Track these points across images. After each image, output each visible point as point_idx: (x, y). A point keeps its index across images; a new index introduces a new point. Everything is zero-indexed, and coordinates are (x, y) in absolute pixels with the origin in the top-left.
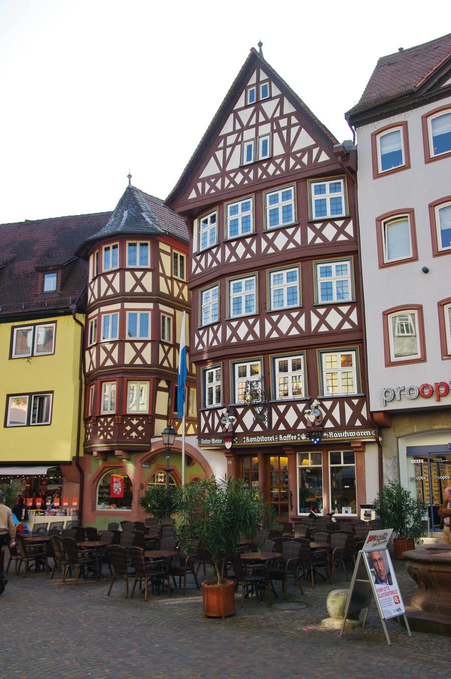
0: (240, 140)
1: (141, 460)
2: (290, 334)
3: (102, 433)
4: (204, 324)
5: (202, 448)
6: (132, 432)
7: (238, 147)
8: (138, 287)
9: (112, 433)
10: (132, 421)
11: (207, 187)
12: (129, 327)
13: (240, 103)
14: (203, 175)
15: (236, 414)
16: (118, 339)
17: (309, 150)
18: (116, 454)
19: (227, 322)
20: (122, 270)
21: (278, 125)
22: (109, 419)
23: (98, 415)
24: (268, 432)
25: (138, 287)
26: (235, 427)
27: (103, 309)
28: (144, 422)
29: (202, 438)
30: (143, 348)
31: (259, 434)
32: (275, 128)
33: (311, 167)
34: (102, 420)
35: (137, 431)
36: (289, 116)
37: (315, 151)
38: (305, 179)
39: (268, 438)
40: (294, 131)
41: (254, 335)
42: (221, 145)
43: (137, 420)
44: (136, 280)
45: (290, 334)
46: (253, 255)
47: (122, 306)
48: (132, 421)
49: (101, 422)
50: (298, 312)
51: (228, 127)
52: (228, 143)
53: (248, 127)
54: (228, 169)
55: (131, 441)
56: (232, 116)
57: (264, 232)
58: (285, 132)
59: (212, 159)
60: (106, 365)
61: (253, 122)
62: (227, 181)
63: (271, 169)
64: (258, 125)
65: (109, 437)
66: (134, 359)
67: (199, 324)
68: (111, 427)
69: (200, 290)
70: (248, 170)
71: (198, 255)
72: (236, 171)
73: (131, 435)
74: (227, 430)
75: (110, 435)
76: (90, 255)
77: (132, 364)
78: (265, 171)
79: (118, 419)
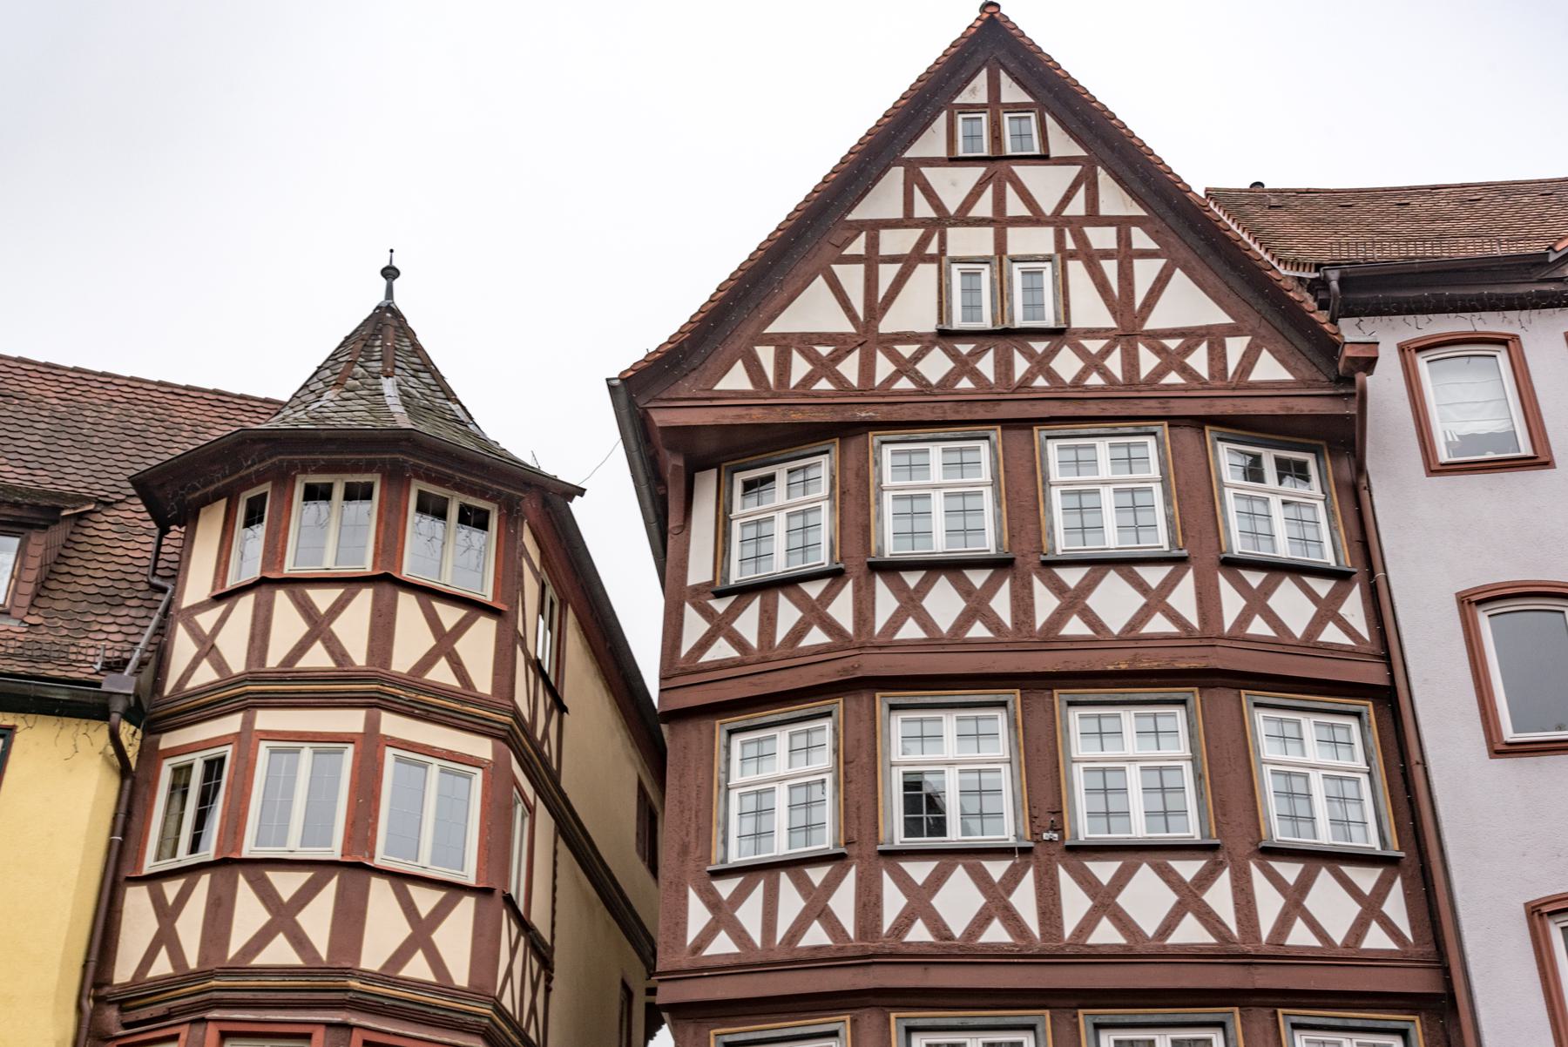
0: (933, 248)
2: (1174, 939)
4: (735, 858)
7: (926, 274)
8: (443, 663)
11: (800, 368)
13: (932, 143)
14: (782, 325)
16: (336, 855)
17: (1214, 337)
20: (387, 581)
21: (1081, 239)
25: (443, 663)
27: (266, 720)
30: (440, 913)
32: (1070, 244)
33: (1226, 388)
36: (1122, 224)
37: (1235, 348)
38: (1199, 422)
40: (1145, 273)
41: (1012, 920)
42: (858, 246)
44: (435, 635)
45: (1174, 939)
46: (999, 630)
47: (372, 725)
50: (1204, 862)
51: (884, 200)
52: (885, 249)
53: (963, 219)
54: (889, 324)
56: (897, 175)
57: (1043, 558)
58: (1110, 268)
59: (820, 281)
60: (260, 960)
61: (984, 207)
62: (884, 368)
63: (1067, 365)
64: (1000, 222)
66: (402, 956)
67: (717, 854)
69: (720, 726)
70: (972, 346)
71: (720, 594)
72: (925, 343)
76: (208, 500)
77: (387, 976)
78: (1041, 365)
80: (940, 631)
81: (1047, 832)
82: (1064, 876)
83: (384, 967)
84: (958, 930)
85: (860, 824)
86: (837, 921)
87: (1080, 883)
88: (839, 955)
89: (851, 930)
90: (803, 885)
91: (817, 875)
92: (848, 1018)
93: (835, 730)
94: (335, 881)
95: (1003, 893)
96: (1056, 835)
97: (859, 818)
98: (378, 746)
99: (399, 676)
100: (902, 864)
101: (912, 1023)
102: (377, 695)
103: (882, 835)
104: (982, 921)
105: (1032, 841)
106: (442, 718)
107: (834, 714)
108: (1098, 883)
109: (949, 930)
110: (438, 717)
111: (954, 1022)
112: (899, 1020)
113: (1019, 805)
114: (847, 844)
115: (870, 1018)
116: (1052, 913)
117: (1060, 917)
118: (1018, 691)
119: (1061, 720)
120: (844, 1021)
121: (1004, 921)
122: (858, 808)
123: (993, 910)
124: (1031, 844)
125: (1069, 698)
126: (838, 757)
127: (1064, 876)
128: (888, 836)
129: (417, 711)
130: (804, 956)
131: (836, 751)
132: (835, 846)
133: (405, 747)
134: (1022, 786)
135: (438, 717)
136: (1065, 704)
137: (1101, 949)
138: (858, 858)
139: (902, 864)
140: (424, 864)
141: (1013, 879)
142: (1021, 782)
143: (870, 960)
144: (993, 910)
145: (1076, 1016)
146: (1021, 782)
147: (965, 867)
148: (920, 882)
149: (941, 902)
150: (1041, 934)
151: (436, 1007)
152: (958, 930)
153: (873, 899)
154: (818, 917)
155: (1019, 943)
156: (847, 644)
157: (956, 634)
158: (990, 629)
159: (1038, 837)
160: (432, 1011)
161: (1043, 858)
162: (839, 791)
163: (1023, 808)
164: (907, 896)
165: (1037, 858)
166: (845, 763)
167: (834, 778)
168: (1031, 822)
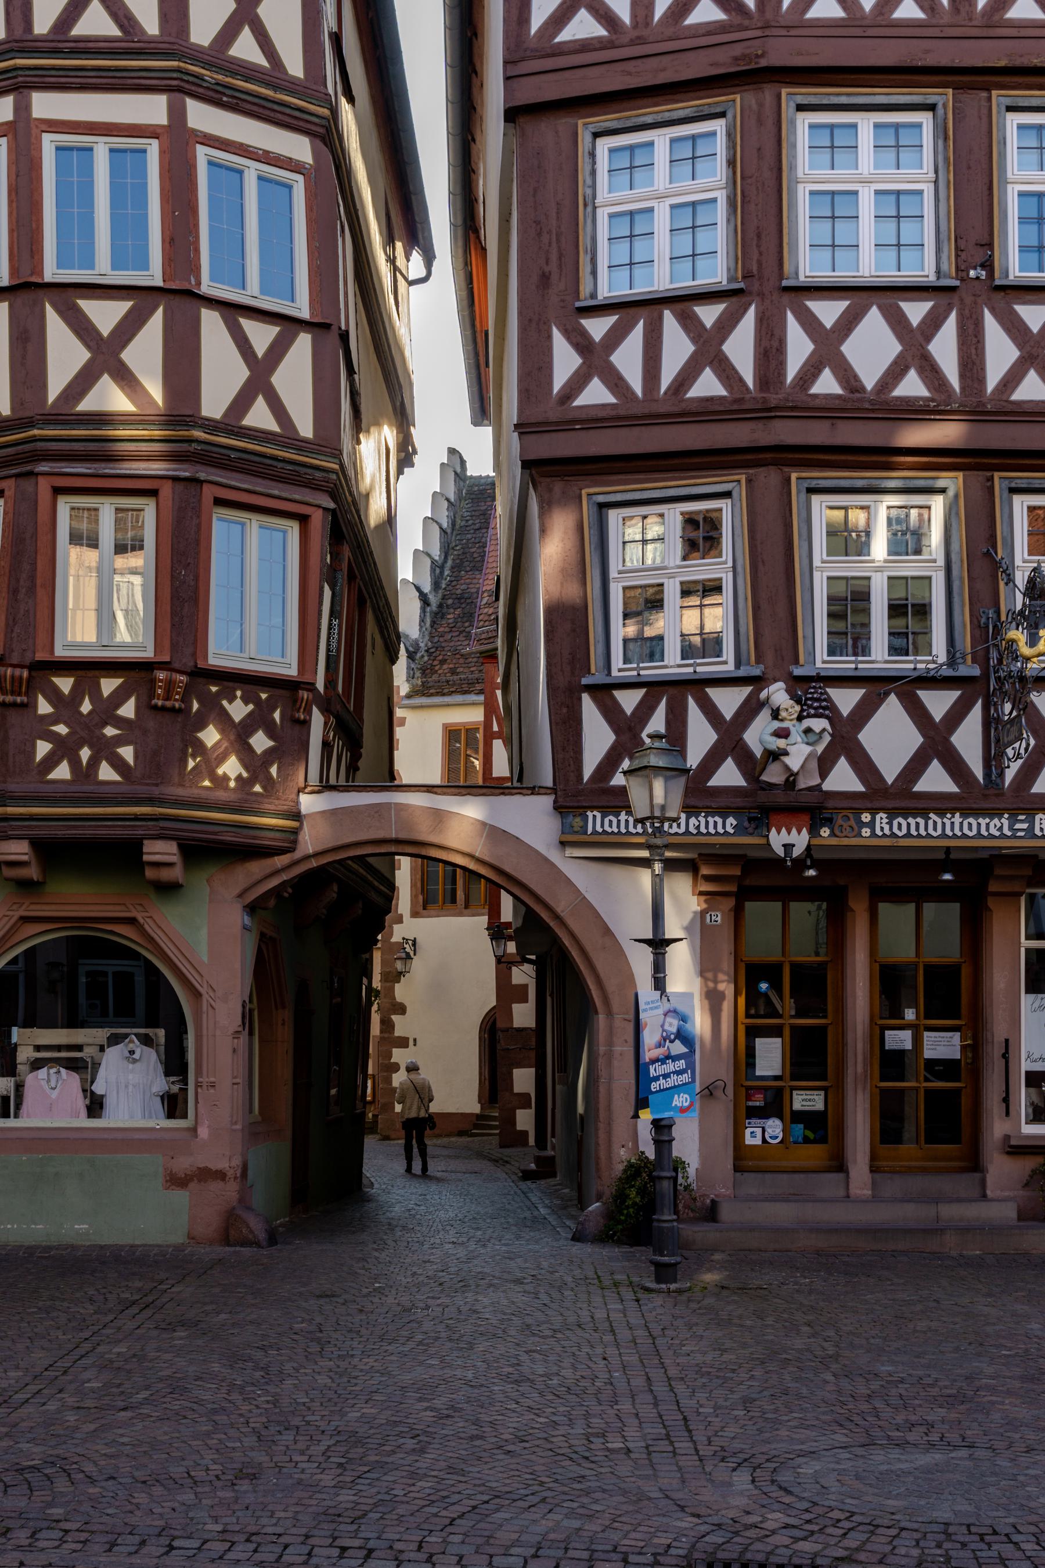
1: (240, 896)
3: (64, 749)
5: (570, 852)
6: (222, 759)
9: (127, 753)
10: (225, 703)
12: (212, 228)
15: (829, 711)
18: (146, 858)
19: (786, 298)
22: (108, 685)
23: (40, 656)
24: (985, 796)
26: (825, 764)
28: (277, 715)
29: (592, 808)
30: (278, 350)
31: (940, 804)
34: (65, 684)
35: (246, 753)
39: (983, 822)
43: (246, 703)
46: (932, 9)
48: (225, 703)
49: (55, 696)
55: (221, 795)
65: (106, 773)
66: (242, 403)
68: (120, 722)
73: (220, 771)
74: (791, 781)
75: (118, 764)
79: (170, 685)
80: (861, 8)
81: (975, 268)
82: (990, 322)
83: (226, 415)
84: (869, 381)
85: (761, 254)
86: (734, 368)
87: (1008, 331)
88: (735, 407)
89: (749, 380)
90: (690, 324)
91: (709, 314)
92: (743, 478)
93: (730, 135)
94: (159, 314)
95: (921, 339)
96: (984, 273)
97: (758, 246)
98: (187, 143)
99: (198, 49)
100: (809, 304)
101: (813, 484)
102: (175, 75)
103: (787, 268)
104: (895, 373)
105: (957, 279)
106: (255, 108)
107: (729, 115)
108: (1027, 329)
109: (860, 381)
110: (248, 106)
111: (860, 484)
112: (800, 481)
113: (944, 236)
114: (744, 277)
115: (769, 477)
116: (974, 363)
117: (983, 369)
118: (950, 91)
119: (998, 130)
120: (739, 481)
121: (921, 372)
122: (759, 236)
123: (910, 359)
124: (957, 283)
125: (1008, 101)
126: (734, 173)
127: (990, 322)
128: (792, 270)
129: (225, 99)
130: (693, 407)
131: (731, 163)
132: (731, 279)
133: (217, 144)
134: (949, 212)
135: (248, 106)
136: (1003, 108)
137: (1025, 406)
138: (758, 295)
139: (809, 304)
140: (252, 293)
141: (933, 324)
142: (949, 206)
143: (773, 414)
144: (910, 359)
145: (991, 479)
146: (949, 206)
147: (880, 308)
148: (828, 324)
149: (851, 349)
150: (963, 388)
151: (284, 460)
152: (869, 381)
153: (775, 344)
154: (711, 364)
155: (936, 397)
156: (746, 23)
157: (881, 14)
158: (922, 8)
159: (964, 274)
160: (280, 465)
161: (969, 300)
162: (735, 211)
163: (949, 239)
164: (814, 341)
165: (962, 300)
166: (742, 178)
167: (728, 197)
168: (957, 256)
